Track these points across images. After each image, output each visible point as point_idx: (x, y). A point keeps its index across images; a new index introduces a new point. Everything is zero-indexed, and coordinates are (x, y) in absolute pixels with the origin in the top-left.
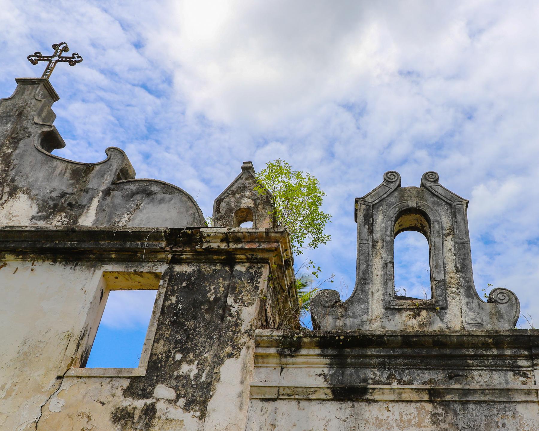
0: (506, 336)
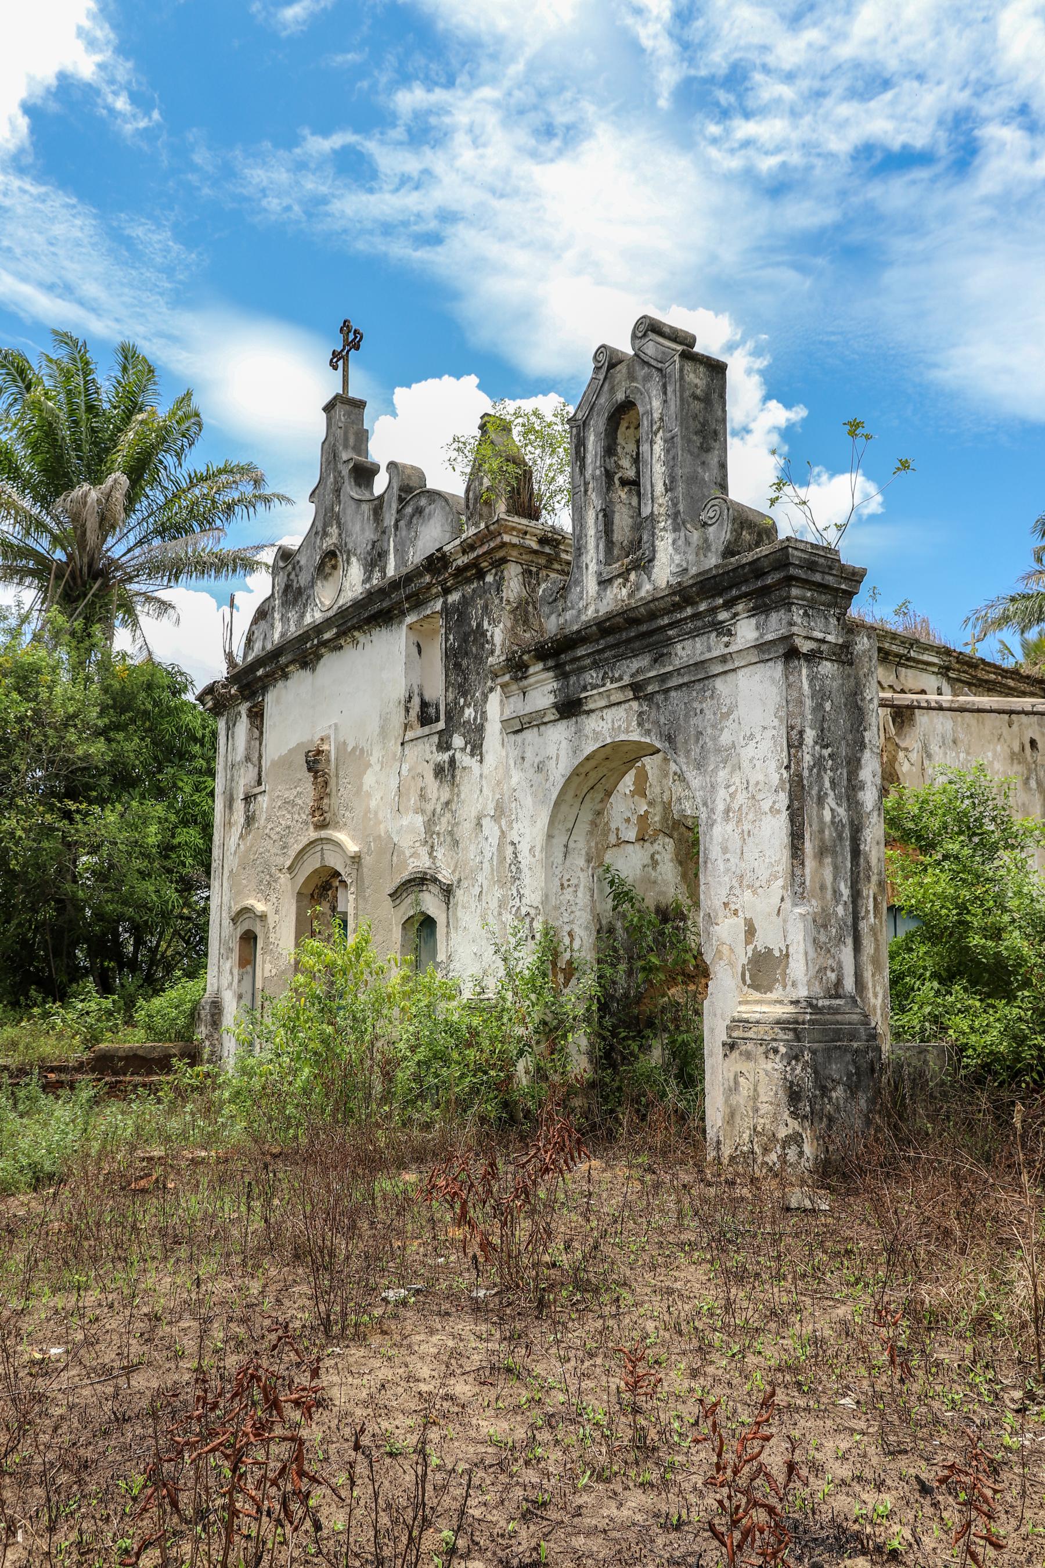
0: (691, 586)
